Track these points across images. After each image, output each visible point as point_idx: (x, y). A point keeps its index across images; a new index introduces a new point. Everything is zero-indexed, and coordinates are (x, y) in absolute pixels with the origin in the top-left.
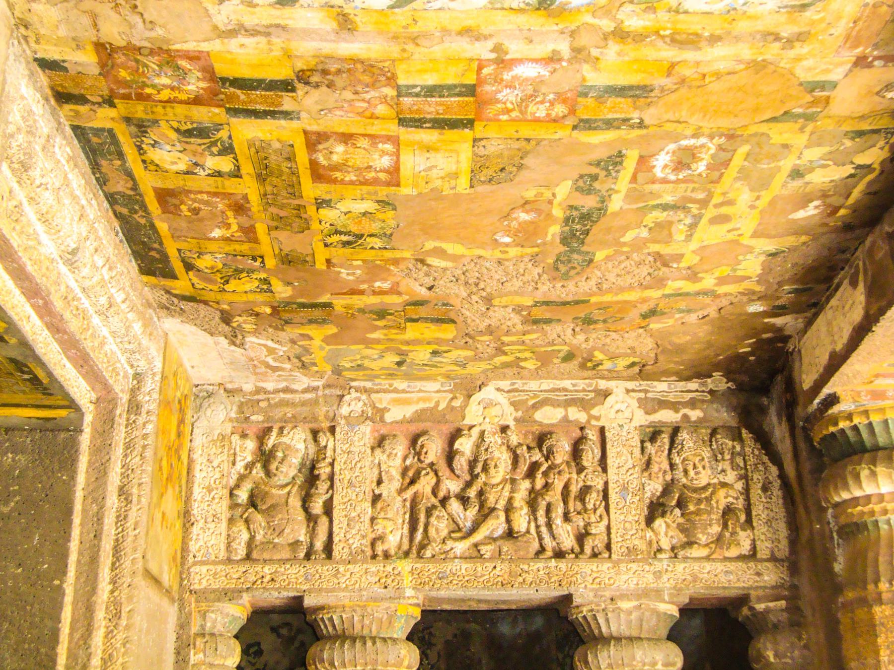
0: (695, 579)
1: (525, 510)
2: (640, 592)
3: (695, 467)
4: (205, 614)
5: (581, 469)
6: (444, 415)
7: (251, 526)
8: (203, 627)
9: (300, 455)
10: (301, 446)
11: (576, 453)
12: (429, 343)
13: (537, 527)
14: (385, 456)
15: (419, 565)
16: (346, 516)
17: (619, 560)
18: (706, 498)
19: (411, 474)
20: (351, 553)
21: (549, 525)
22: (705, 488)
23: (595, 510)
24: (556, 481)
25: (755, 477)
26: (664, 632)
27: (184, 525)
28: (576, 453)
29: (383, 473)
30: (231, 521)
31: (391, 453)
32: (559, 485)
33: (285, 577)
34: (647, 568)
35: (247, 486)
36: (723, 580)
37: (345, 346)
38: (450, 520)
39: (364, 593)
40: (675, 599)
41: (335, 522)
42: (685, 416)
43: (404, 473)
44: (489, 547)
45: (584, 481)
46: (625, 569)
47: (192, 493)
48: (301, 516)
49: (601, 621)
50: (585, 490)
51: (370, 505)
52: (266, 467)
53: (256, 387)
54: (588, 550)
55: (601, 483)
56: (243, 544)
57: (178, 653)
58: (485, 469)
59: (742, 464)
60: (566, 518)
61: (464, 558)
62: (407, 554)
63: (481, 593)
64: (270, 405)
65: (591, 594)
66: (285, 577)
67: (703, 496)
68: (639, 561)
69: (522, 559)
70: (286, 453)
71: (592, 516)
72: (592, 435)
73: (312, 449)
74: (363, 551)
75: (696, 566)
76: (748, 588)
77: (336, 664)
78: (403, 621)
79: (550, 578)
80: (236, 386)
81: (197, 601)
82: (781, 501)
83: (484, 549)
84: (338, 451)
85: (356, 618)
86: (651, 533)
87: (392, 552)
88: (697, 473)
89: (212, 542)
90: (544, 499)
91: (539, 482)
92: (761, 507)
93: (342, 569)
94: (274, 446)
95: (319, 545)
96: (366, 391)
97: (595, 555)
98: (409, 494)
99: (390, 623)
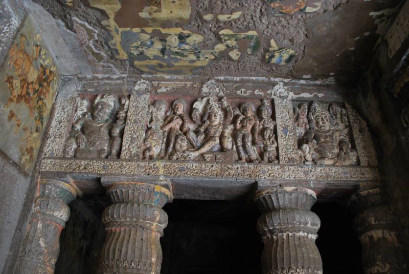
0: (327, 176)
1: (230, 139)
2: (297, 182)
3: (322, 120)
4: (45, 185)
5: (261, 119)
6: (189, 91)
7: (78, 141)
8: (43, 192)
9: (111, 109)
10: (112, 104)
11: (259, 113)
12: (177, 25)
13: (237, 147)
14: (155, 109)
15: (168, 163)
16: (130, 137)
17: (284, 164)
18: (329, 135)
19: (169, 119)
20: (131, 156)
21: (244, 146)
22: (329, 131)
23: (270, 138)
24: (248, 124)
25: (355, 125)
26: (309, 208)
27: (43, 139)
28: (259, 113)
29: (153, 117)
30: (68, 139)
31: (158, 108)
32: (249, 127)
33: (92, 167)
34: (300, 169)
35: (81, 122)
36: (344, 177)
37: (128, 29)
38: (189, 142)
39: (136, 177)
40: (317, 186)
41: (124, 140)
42: (316, 96)
43: (165, 119)
44: (210, 155)
45: (263, 125)
46: (287, 169)
47: (51, 123)
48: (106, 137)
49: (274, 198)
50: (264, 129)
51: (144, 132)
52: (92, 115)
53: (93, 76)
54: (266, 159)
55: (273, 126)
56: (73, 150)
57: (25, 205)
58: (209, 118)
59: (347, 120)
60: (254, 143)
61: (195, 161)
62: (162, 158)
63: (204, 179)
64: (99, 85)
65: (268, 182)
66: (92, 167)
67: (328, 134)
68: (295, 165)
69: (229, 162)
70: (103, 106)
71: (268, 142)
72: (267, 103)
73: (118, 106)
74: (138, 155)
75: (328, 169)
76: (358, 181)
77: (115, 216)
78: (158, 196)
79: (244, 173)
80: (83, 75)
81: (41, 178)
82: (370, 137)
83: (206, 156)
84: (131, 106)
85: (130, 192)
86: (301, 152)
87: (155, 156)
88: (323, 123)
89: (56, 148)
90: (241, 132)
91: (239, 126)
92: (360, 140)
93: (124, 164)
94: (98, 104)
95: (114, 152)
96: (148, 79)
97: (270, 162)
98: (167, 129)
99: (150, 196)
